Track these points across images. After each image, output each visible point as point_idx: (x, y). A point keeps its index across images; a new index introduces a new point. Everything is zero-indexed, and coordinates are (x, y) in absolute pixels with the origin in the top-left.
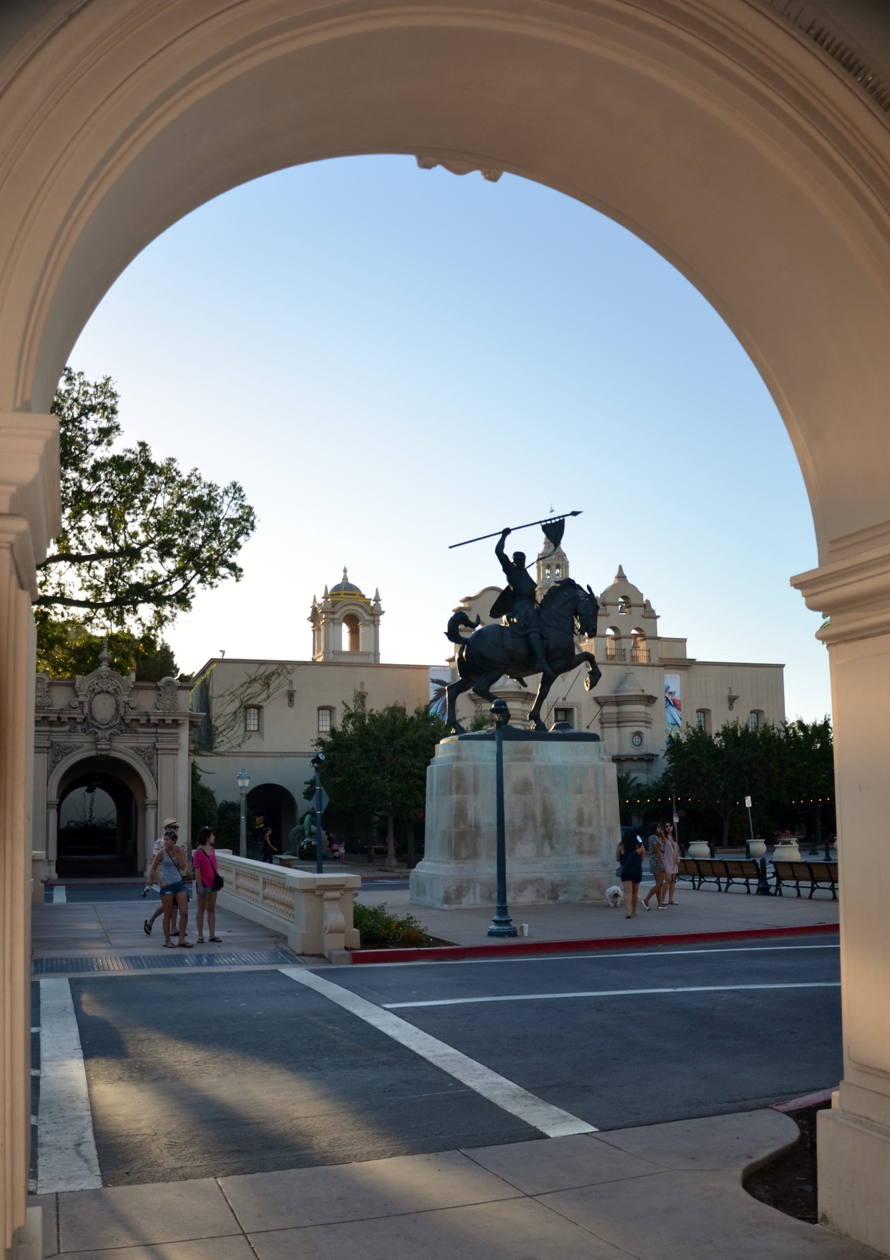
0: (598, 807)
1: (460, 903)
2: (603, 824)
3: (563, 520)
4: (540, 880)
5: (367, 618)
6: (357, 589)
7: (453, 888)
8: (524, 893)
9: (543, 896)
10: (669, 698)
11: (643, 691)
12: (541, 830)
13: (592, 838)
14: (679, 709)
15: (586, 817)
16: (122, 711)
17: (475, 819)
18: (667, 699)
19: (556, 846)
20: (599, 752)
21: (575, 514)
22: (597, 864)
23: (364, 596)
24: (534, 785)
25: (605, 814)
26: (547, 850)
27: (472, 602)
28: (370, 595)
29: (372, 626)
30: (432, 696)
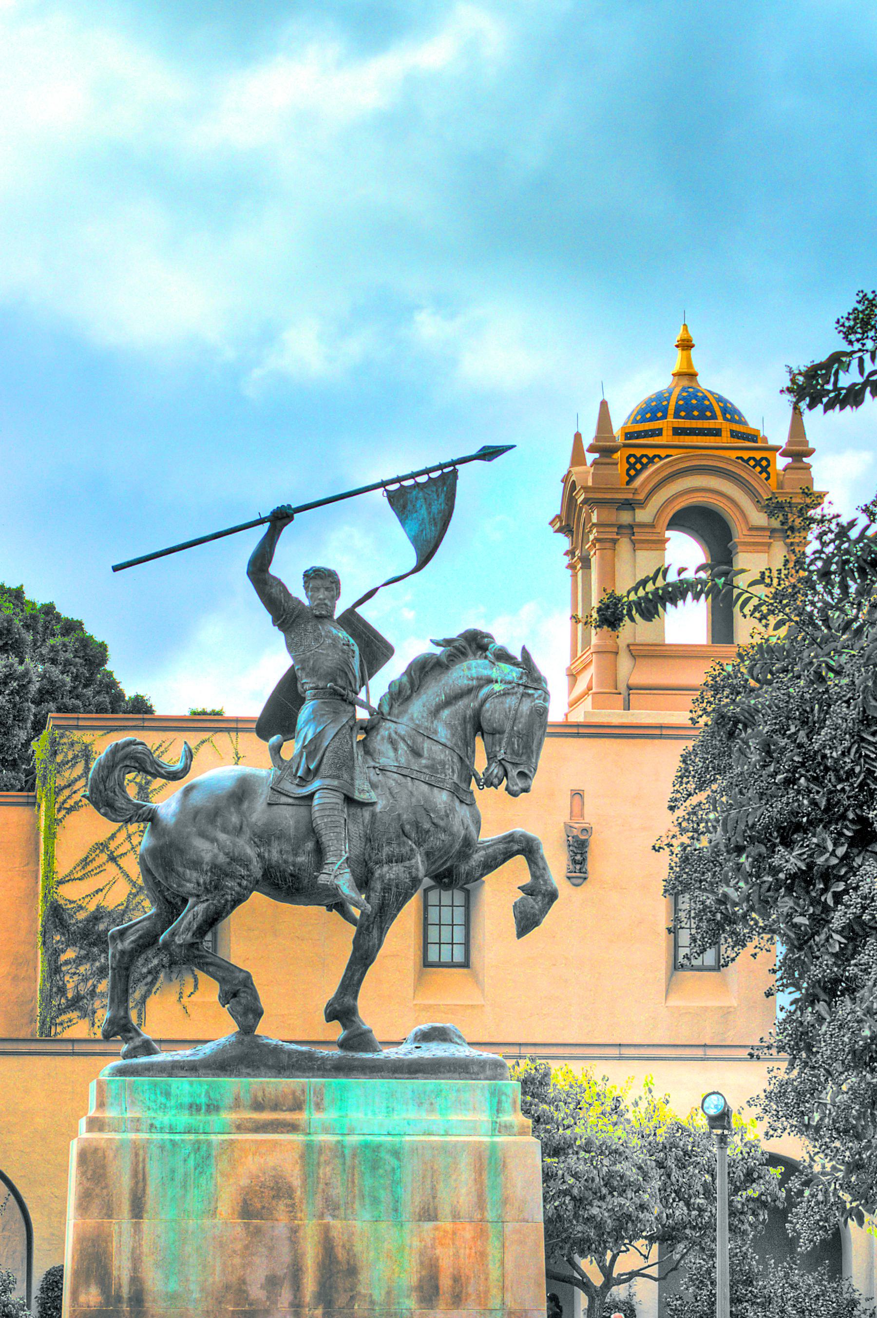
3: (455, 473)
5: (759, 518)
15: (445, 1282)
21: (489, 454)
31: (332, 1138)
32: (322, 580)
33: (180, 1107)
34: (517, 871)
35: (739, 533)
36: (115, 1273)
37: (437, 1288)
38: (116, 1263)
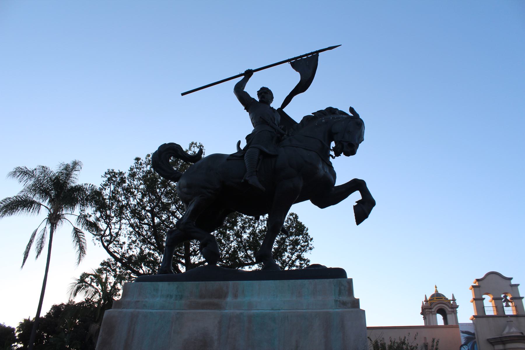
5: (450, 310)
6: (443, 295)
23: (447, 299)
27: (481, 282)
28: (450, 298)
29: (453, 314)
30: (463, 341)
31: (238, 312)
32: (266, 94)
35: (447, 312)
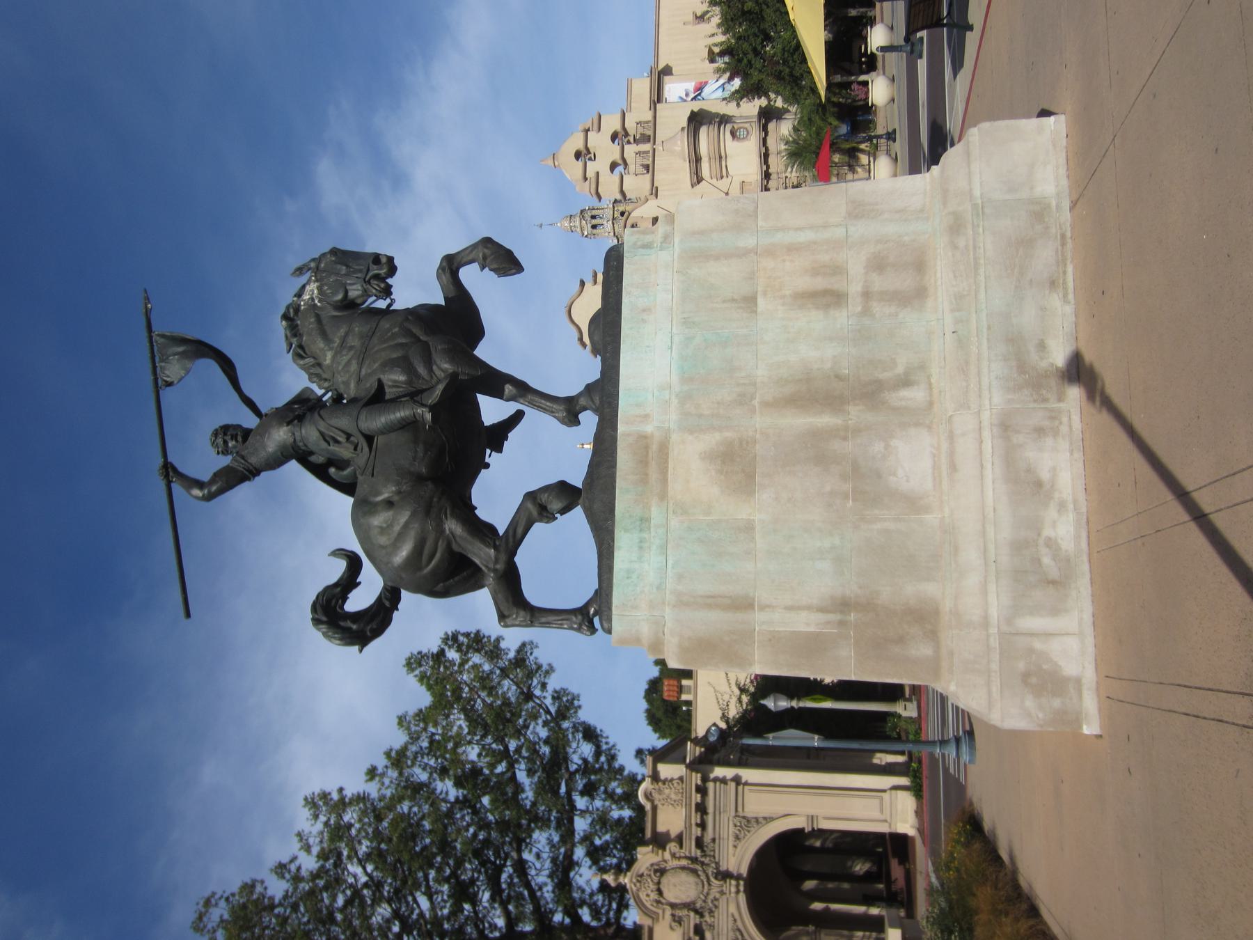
0: (792, 249)
1: (1078, 681)
2: (839, 232)
4: (1005, 426)
7: (1030, 703)
8: (1045, 476)
9: (1054, 416)
10: (692, 95)
11: (683, 129)
12: (856, 414)
13: (878, 264)
14: (706, 83)
15: (820, 283)
16: (684, 862)
17: (822, 610)
18: (694, 98)
19: (900, 369)
20: (647, 246)
22: (955, 247)
24: (728, 434)
25: (811, 227)
26: (914, 395)
31: (675, 402)
33: (640, 558)
34: (471, 276)
36: (812, 629)
37: (826, 293)
38: (803, 628)
